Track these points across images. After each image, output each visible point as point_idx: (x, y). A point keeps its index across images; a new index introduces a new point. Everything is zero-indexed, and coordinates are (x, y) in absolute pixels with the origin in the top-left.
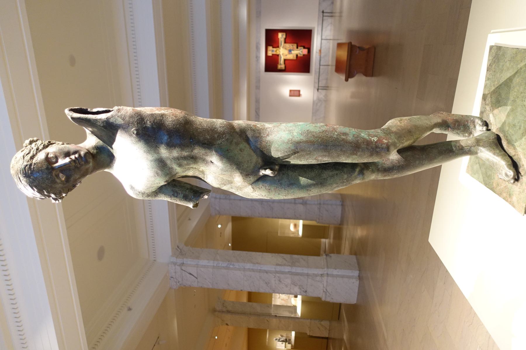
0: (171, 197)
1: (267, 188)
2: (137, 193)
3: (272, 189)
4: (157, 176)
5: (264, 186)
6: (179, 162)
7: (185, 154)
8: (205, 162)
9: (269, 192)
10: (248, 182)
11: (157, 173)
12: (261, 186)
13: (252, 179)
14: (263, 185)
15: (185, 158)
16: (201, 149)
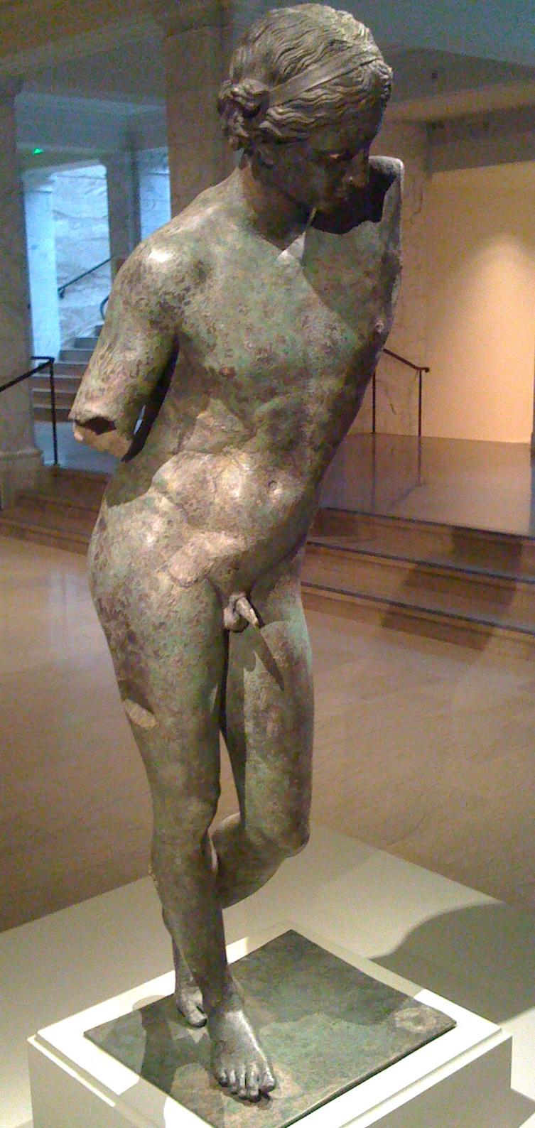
0: (148, 364)
1: (204, 615)
2: (183, 280)
3: (201, 629)
4: (258, 357)
5: (206, 606)
6: (289, 413)
7: (309, 430)
8: (271, 468)
9: (190, 621)
10: (213, 570)
11: (268, 360)
12: (206, 599)
13: (225, 577)
14: (207, 605)
15: (298, 427)
16: (314, 463)
